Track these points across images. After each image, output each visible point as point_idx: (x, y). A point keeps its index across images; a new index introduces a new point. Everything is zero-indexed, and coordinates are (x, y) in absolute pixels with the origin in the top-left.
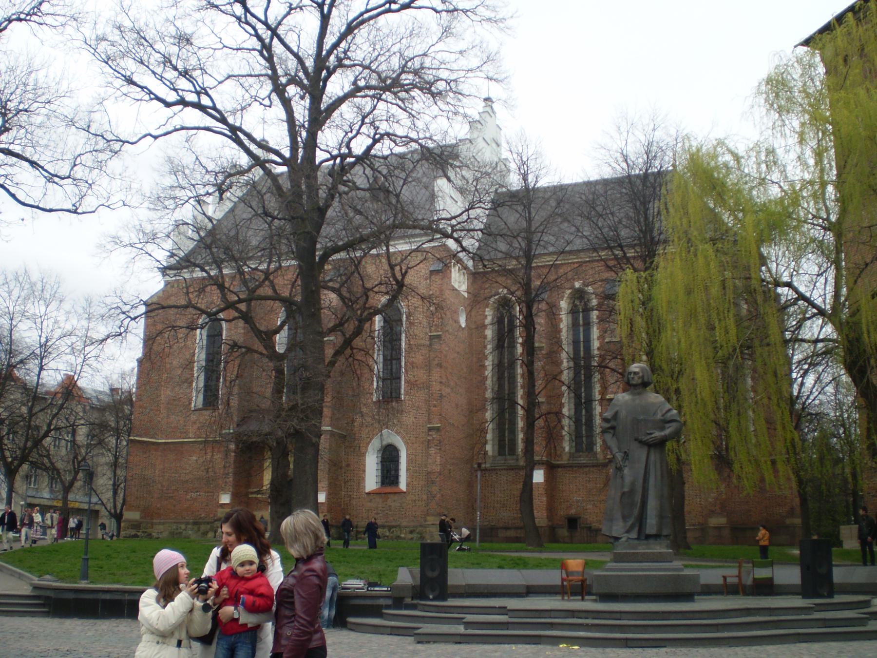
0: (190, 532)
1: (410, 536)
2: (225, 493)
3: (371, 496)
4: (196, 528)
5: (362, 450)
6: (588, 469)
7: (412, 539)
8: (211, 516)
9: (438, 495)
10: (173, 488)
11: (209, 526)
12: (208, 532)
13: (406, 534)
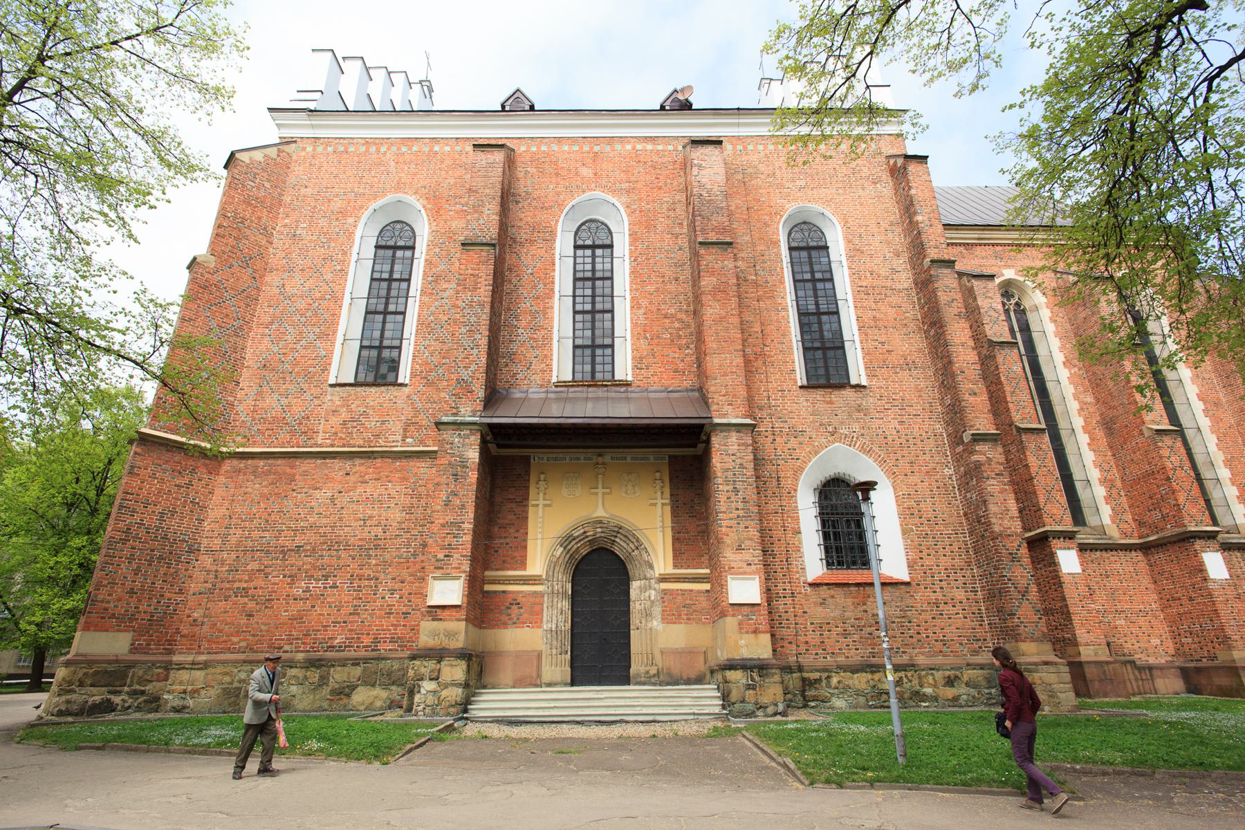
0: (294, 689)
1: (950, 692)
2: (447, 577)
3: (824, 592)
4: (314, 675)
5: (787, 483)
6: (1098, 553)
7: (956, 699)
8: (366, 641)
9: (1034, 588)
10: (253, 566)
11: (358, 671)
12: (353, 688)
13: (935, 686)
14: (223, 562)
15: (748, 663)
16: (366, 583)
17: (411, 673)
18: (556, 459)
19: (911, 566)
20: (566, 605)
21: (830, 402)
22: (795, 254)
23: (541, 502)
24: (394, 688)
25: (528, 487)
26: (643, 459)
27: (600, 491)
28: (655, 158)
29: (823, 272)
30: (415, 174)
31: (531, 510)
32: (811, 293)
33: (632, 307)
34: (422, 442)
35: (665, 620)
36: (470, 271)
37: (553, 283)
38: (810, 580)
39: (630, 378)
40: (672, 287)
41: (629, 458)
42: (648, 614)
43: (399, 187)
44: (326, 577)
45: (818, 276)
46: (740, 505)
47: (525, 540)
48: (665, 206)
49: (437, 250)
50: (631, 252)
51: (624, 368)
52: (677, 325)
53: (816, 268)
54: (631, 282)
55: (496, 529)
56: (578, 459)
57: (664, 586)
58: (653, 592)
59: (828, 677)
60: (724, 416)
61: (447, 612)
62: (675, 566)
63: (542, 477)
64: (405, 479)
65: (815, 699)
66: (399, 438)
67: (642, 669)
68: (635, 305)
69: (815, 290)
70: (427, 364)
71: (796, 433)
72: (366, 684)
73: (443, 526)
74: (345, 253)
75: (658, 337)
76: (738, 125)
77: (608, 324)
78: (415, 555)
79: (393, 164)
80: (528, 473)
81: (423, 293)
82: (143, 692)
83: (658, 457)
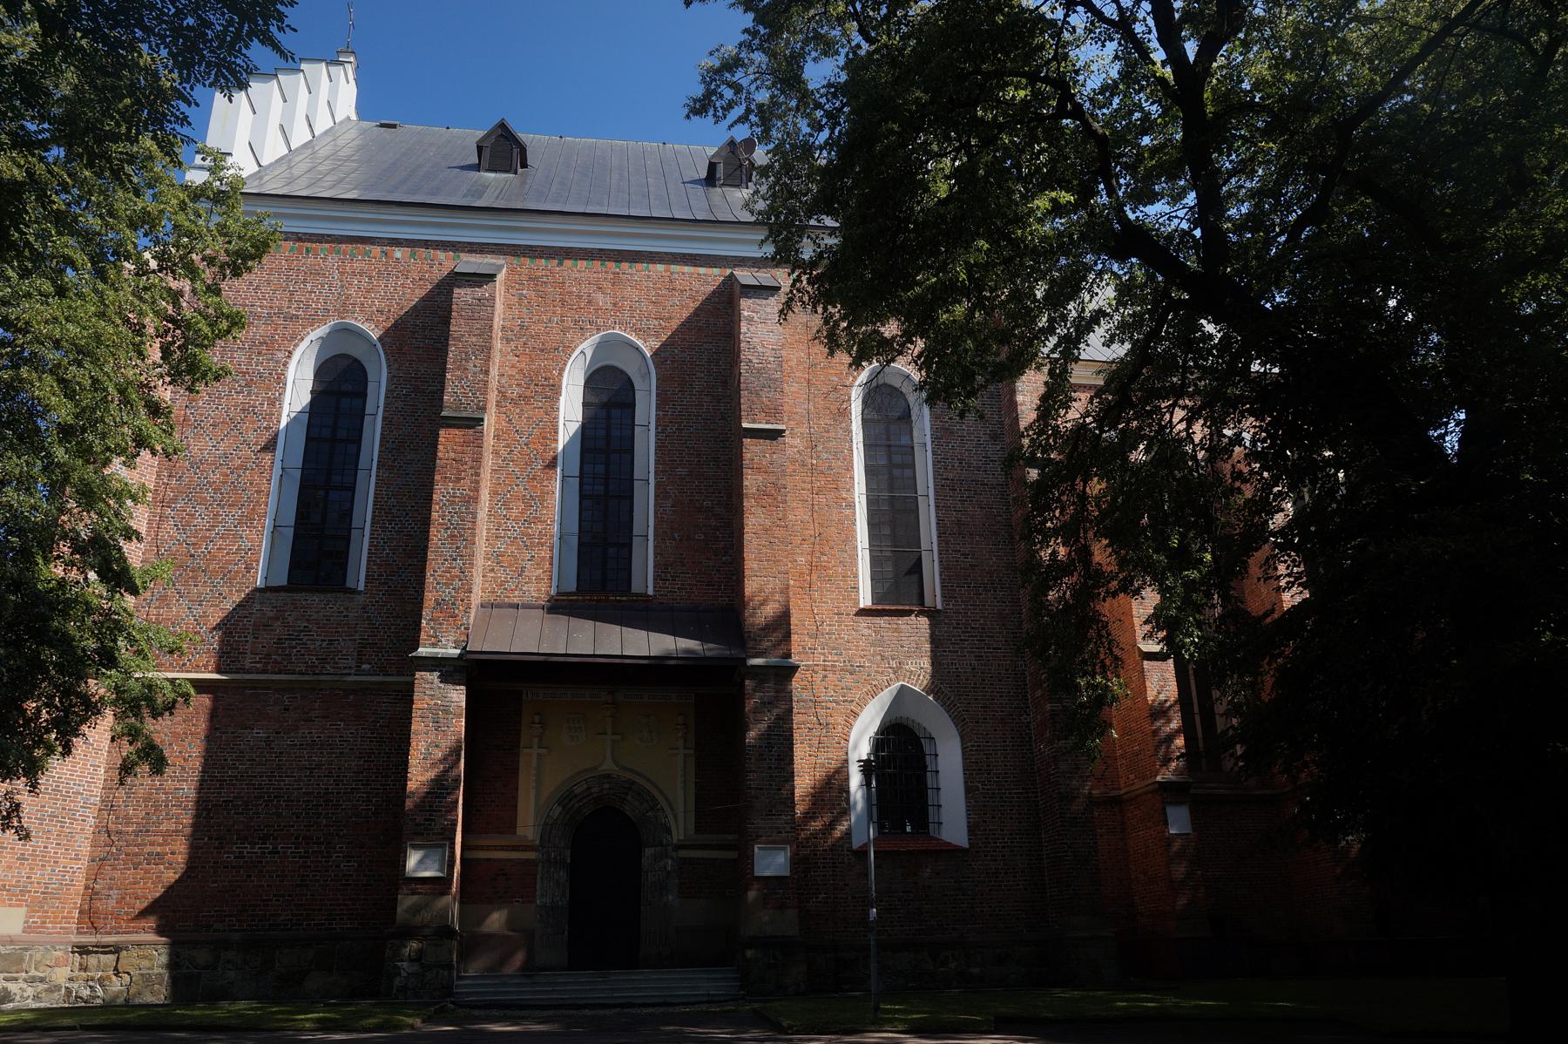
14: (128, 820)
19: (972, 830)
20: (563, 875)
21: (896, 630)
31: (522, 760)
33: (656, 496)
44: (264, 839)
47: (515, 798)
49: (400, 404)
51: (645, 575)
52: (713, 522)
57: (683, 853)
62: (697, 830)
63: (537, 719)
66: (353, 664)
74: (272, 403)
82: (42, 980)
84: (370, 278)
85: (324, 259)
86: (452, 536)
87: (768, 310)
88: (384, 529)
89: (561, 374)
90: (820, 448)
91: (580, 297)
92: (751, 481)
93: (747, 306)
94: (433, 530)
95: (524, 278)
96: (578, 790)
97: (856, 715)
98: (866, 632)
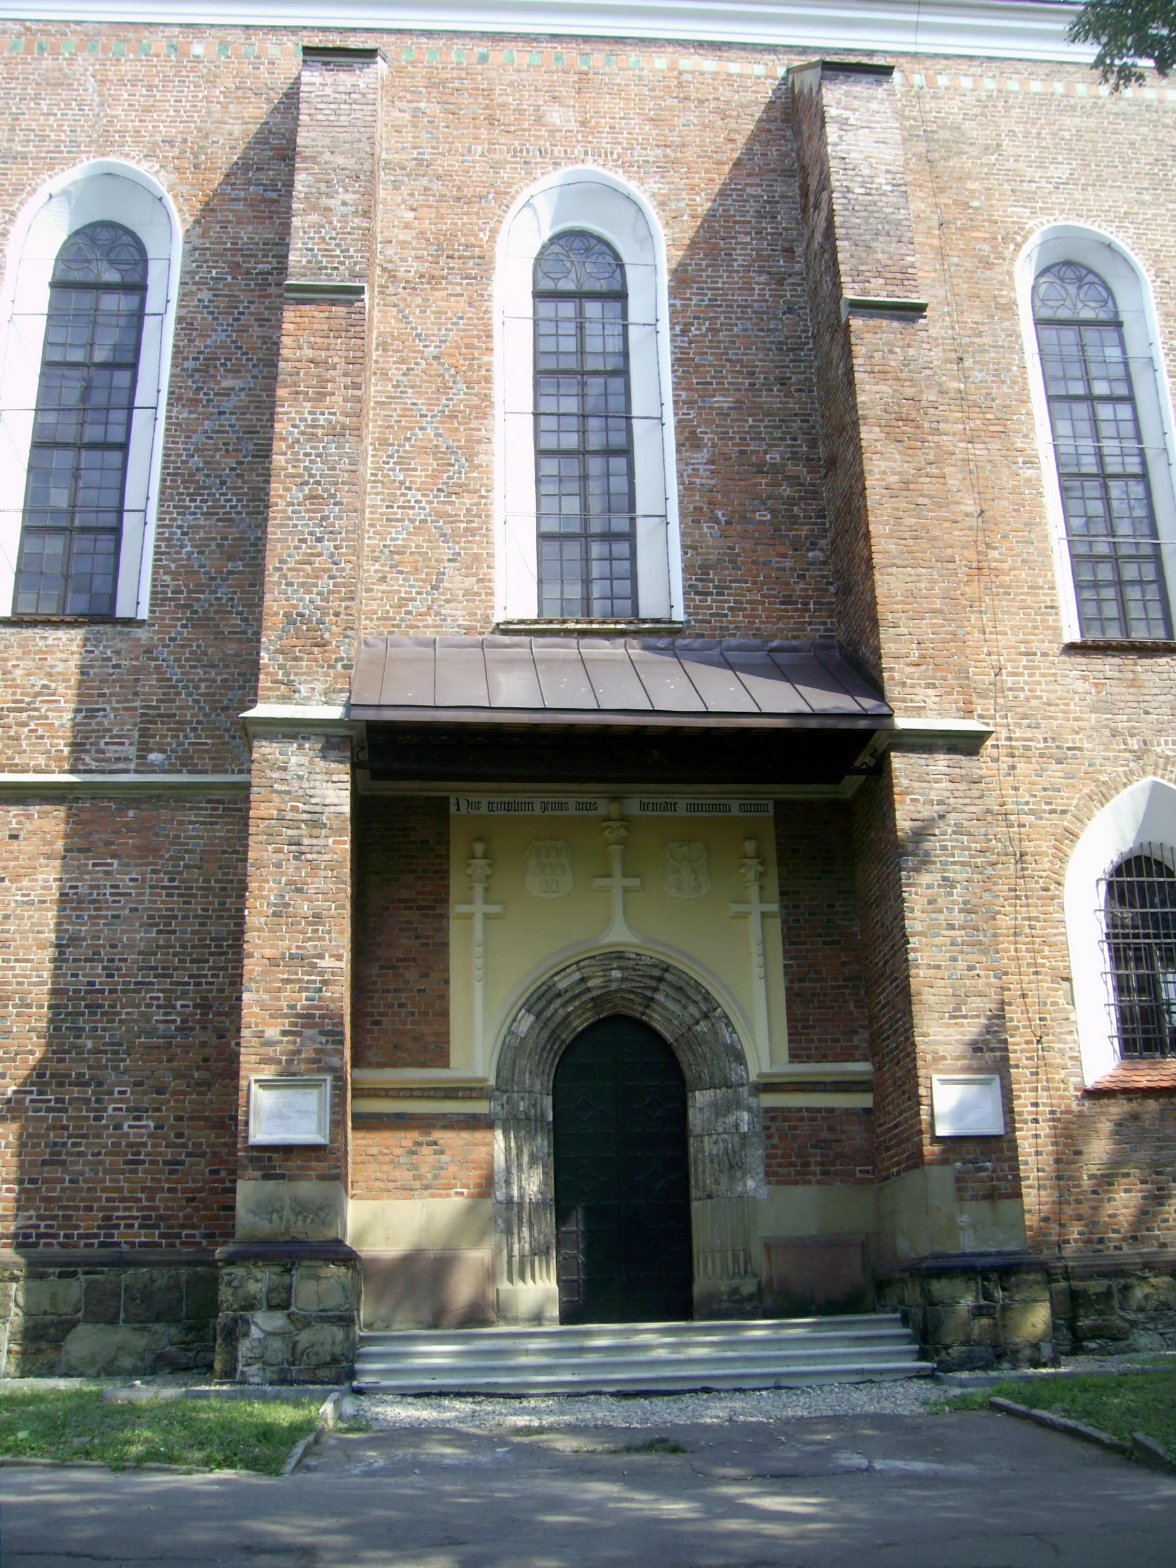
8: (87, 1223)
15: (979, 1262)
16: (76, 1092)
17: (225, 1294)
18: (508, 807)
21: (1134, 683)
22: (1050, 333)
23: (479, 908)
24: (158, 1327)
25: (444, 874)
26: (717, 808)
27: (618, 882)
28: (725, 93)
29: (1110, 380)
30: (147, 110)
31: (455, 929)
32: (1085, 428)
33: (680, 446)
34: (186, 763)
35: (771, 1176)
36: (309, 353)
37: (488, 380)
38: (1089, 1084)
39: (679, 615)
40: (773, 399)
41: (682, 804)
42: (733, 1165)
43: (106, 141)
45: (1100, 388)
46: (958, 918)
47: (444, 997)
48: (752, 207)
49: (205, 295)
50: (674, 312)
52: (786, 491)
53: (1095, 370)
54: (676, 386)
55: (375, 971)
56: (561, 806)
57: (770, 1100)
58: (745, 1116)
59: (1126, 1288)
60: (919, 711)
61: (296, 1162)
62: (795, 1056)
63: (479, 848)
64: (147, 851)
65: (1096, 1333)
66: (132, 751)
67: (724, 1286)
68: (688, 440)
69: (1094, 420)
70: (191, 573)
71: (1060, 753)
72: (94, 1317)
73: (273, 962)
75: (743, 519)
76: (917, 27)
77: (618, 484)
78: (184, 1029)
79: (91, 84)
80: (444, 839)
81: (175, 398)
83: (742, 804)
84: (150, 88)
85: (71, 60)
86: (312, 497)
87: (874, 106)
88: (183, 511)
89: (492, 238)
90: (968, 363)
91: (520, 112)
92: (870, 393)
93: (837, 98)
94: (276, 488)
95: (420, 81)
96: (562, 986)
97: (1073, 836)
98: (1080, 686)
